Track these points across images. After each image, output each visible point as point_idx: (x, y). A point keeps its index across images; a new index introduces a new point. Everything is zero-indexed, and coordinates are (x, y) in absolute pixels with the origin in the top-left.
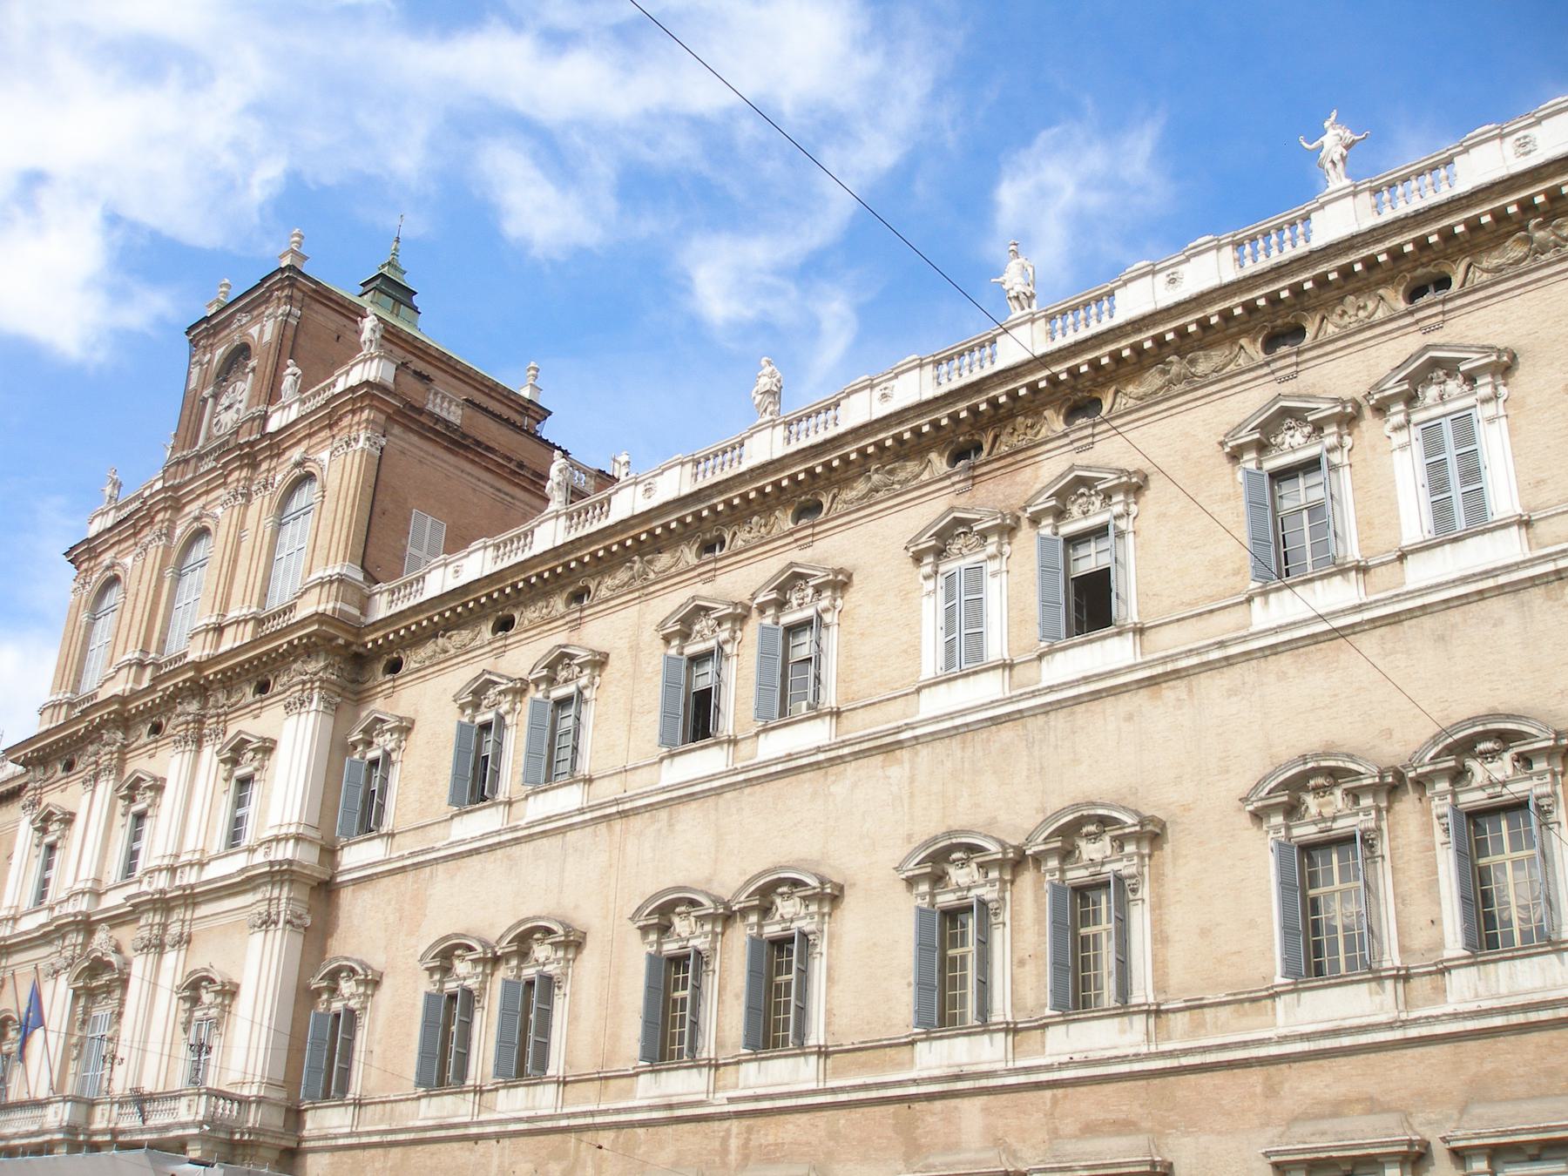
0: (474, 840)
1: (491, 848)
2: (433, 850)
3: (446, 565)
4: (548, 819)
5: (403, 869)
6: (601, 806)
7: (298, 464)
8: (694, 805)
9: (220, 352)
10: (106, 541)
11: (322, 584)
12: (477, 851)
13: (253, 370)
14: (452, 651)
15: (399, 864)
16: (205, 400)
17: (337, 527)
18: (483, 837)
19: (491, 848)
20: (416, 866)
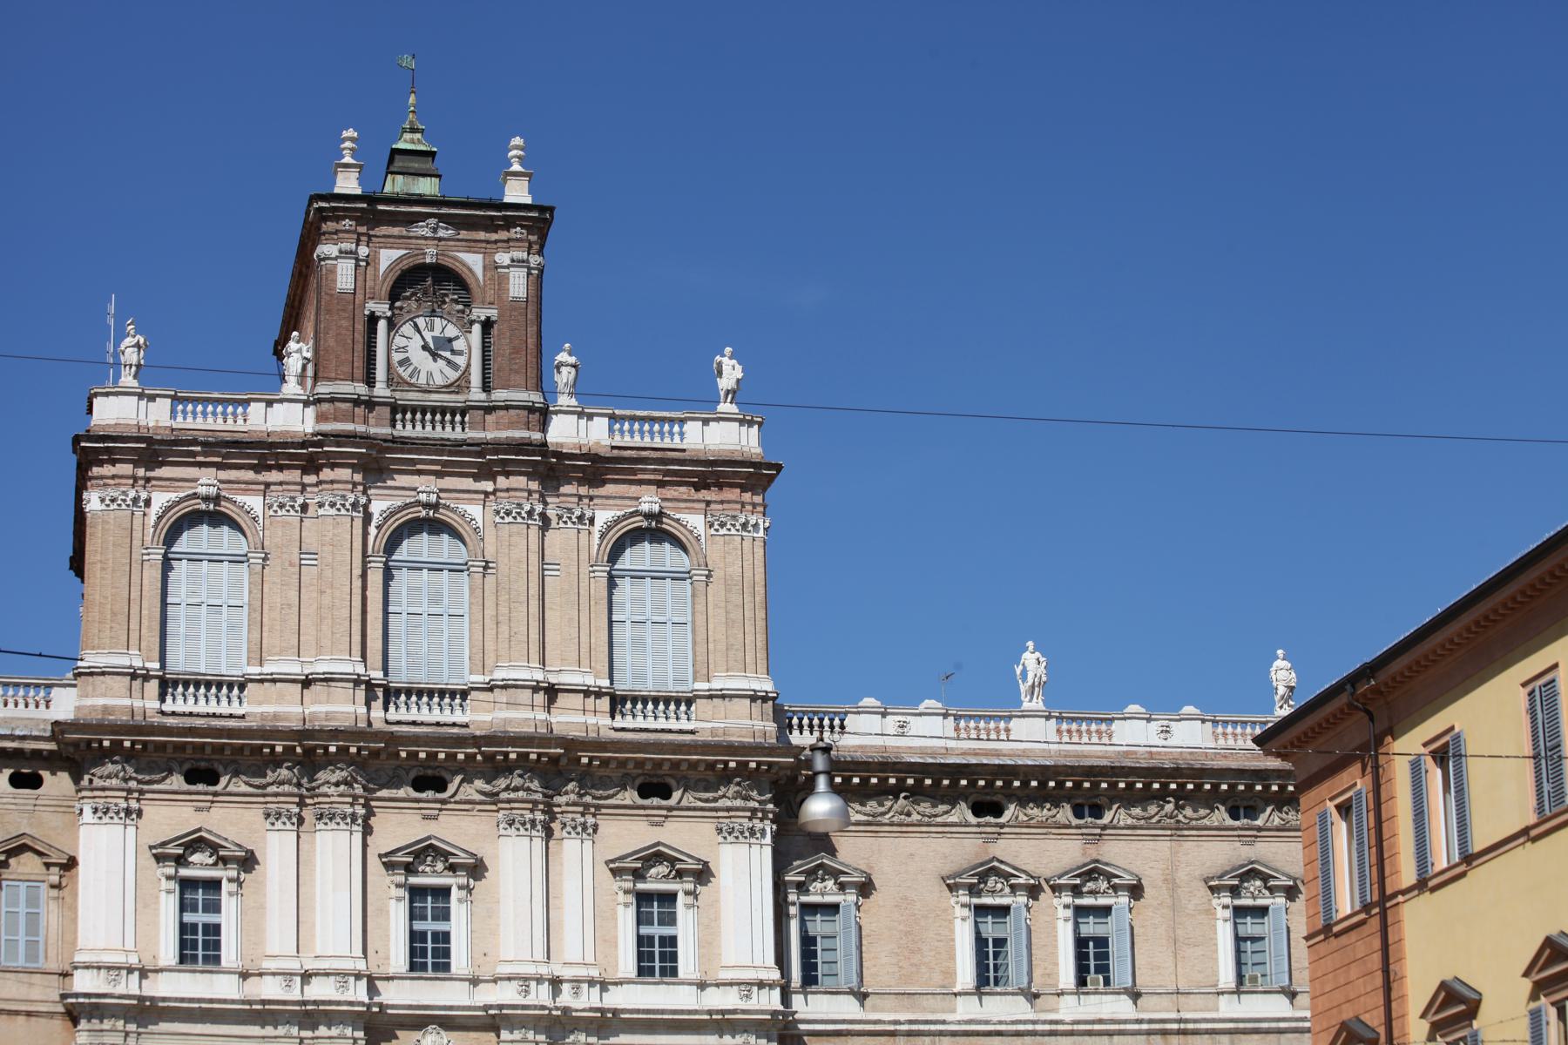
0: (1000, 1022)
1: (1018, 1034)
2: (944, 1022)
3: (884, 715)
4: (1100, 1021)
5: (892, 1034)
6: (1151, 1021)
7: (649, 516)
8: (1256, 1037)
9: (388, 257)
10: (194, 454)
11: (753, 698)
12: (999, 1034)
13: (487, 325)
14: (915, 817)
15: (892, 1028)
16: (373, 320)
17: (749, 628)
18: (1013, 1023)
19: (1018, 1034)
20: (910, 1034)
